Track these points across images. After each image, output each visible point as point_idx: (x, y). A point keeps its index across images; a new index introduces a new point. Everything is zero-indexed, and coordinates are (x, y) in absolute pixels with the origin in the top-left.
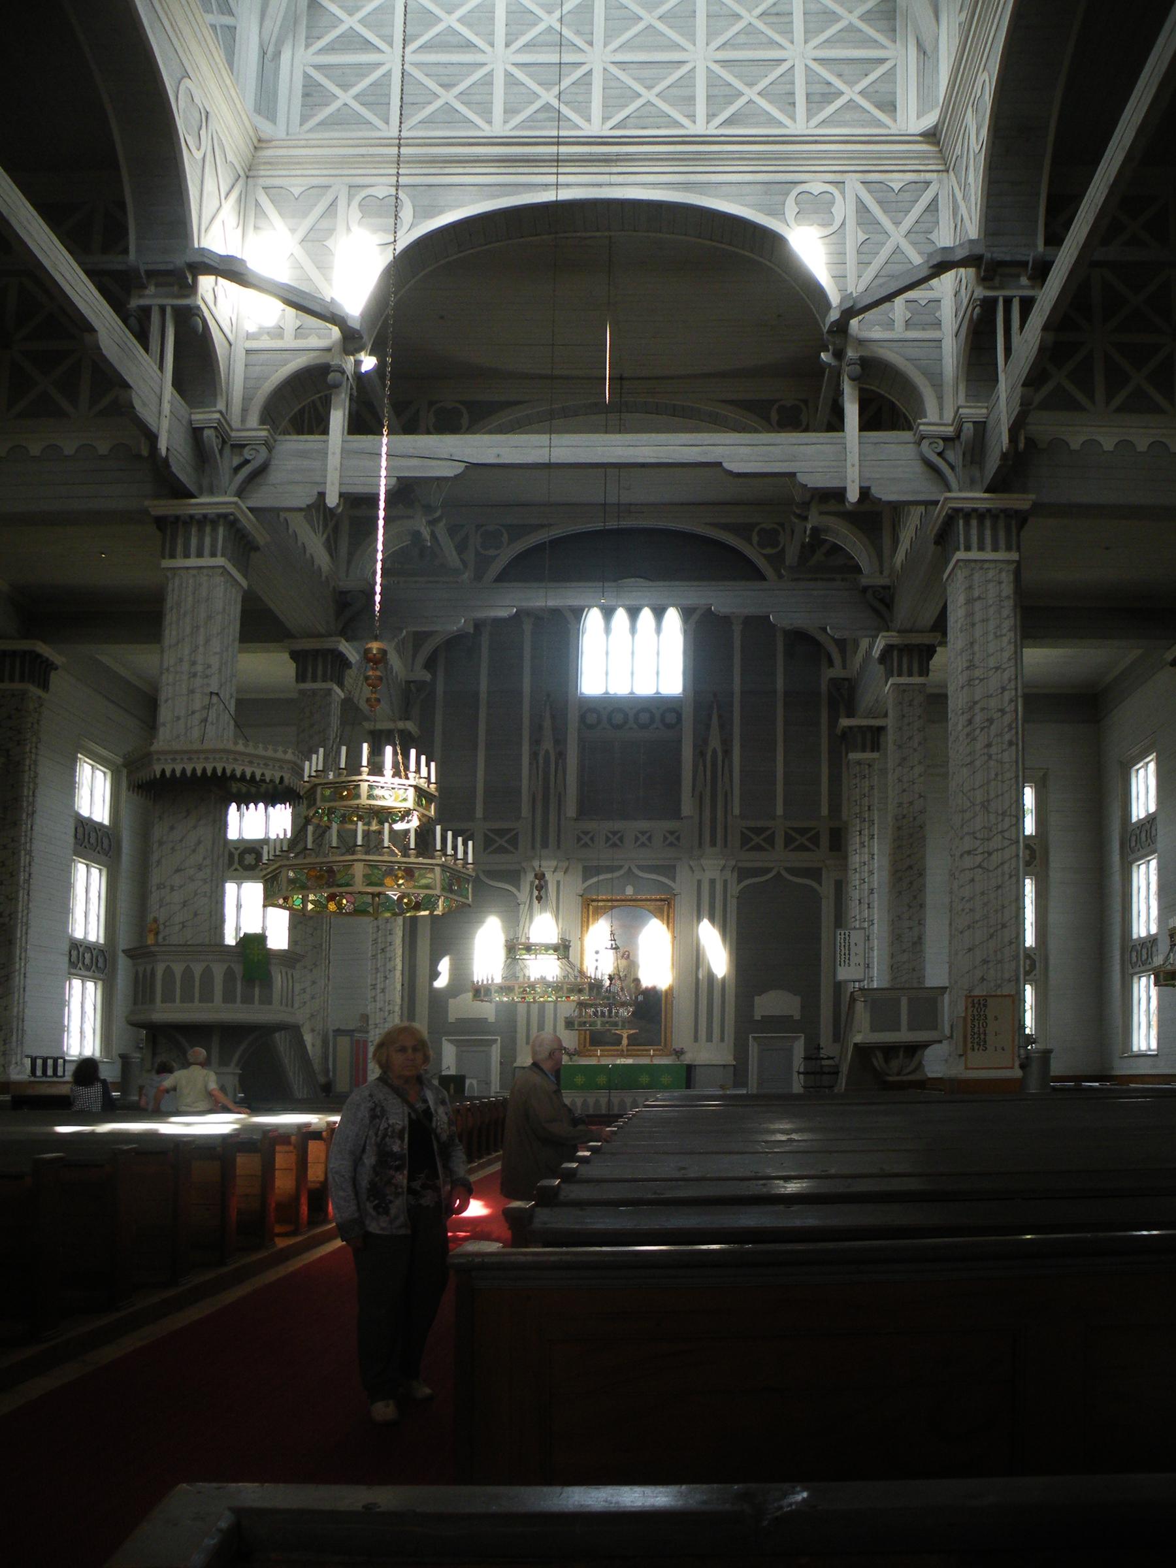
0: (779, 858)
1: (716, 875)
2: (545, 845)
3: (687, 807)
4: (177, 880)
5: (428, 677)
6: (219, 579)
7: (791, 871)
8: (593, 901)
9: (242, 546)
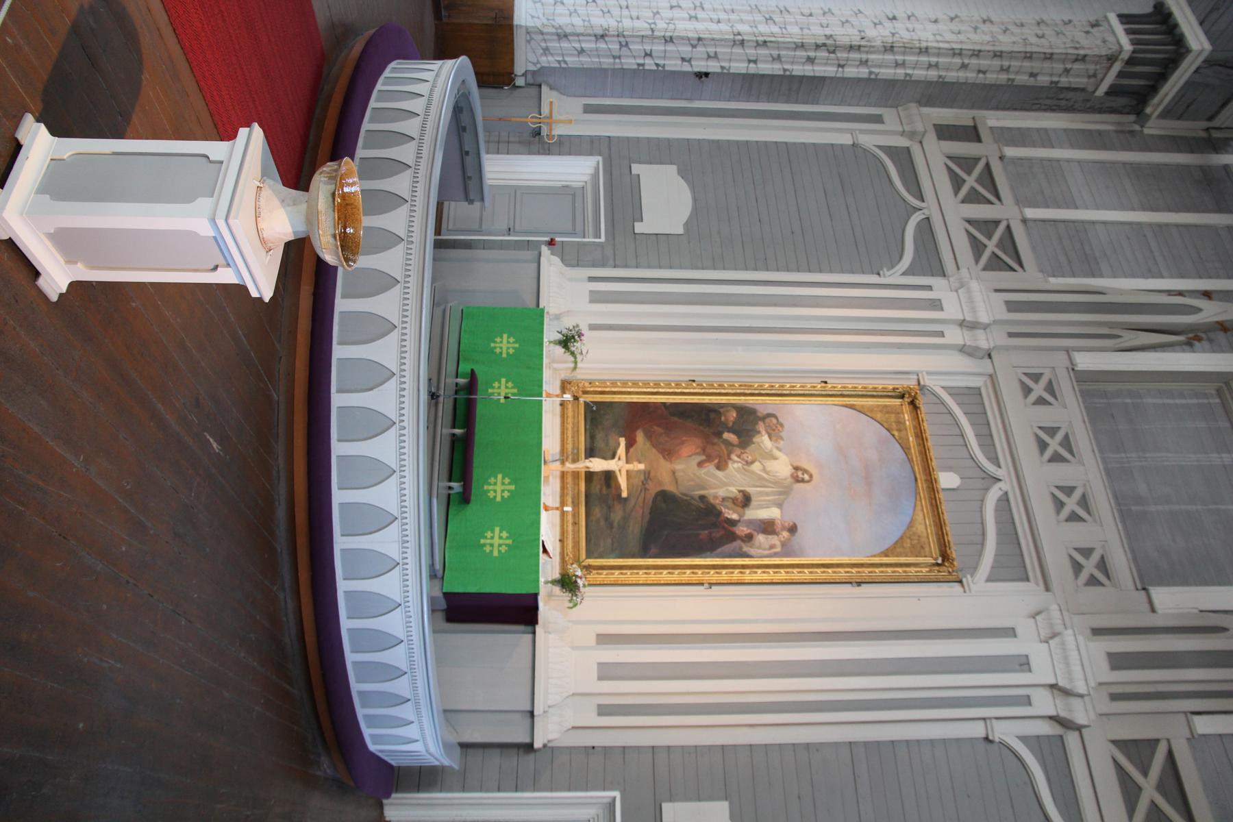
1: (1042, 672)
3: (1173, 601)
8: (913, 403)
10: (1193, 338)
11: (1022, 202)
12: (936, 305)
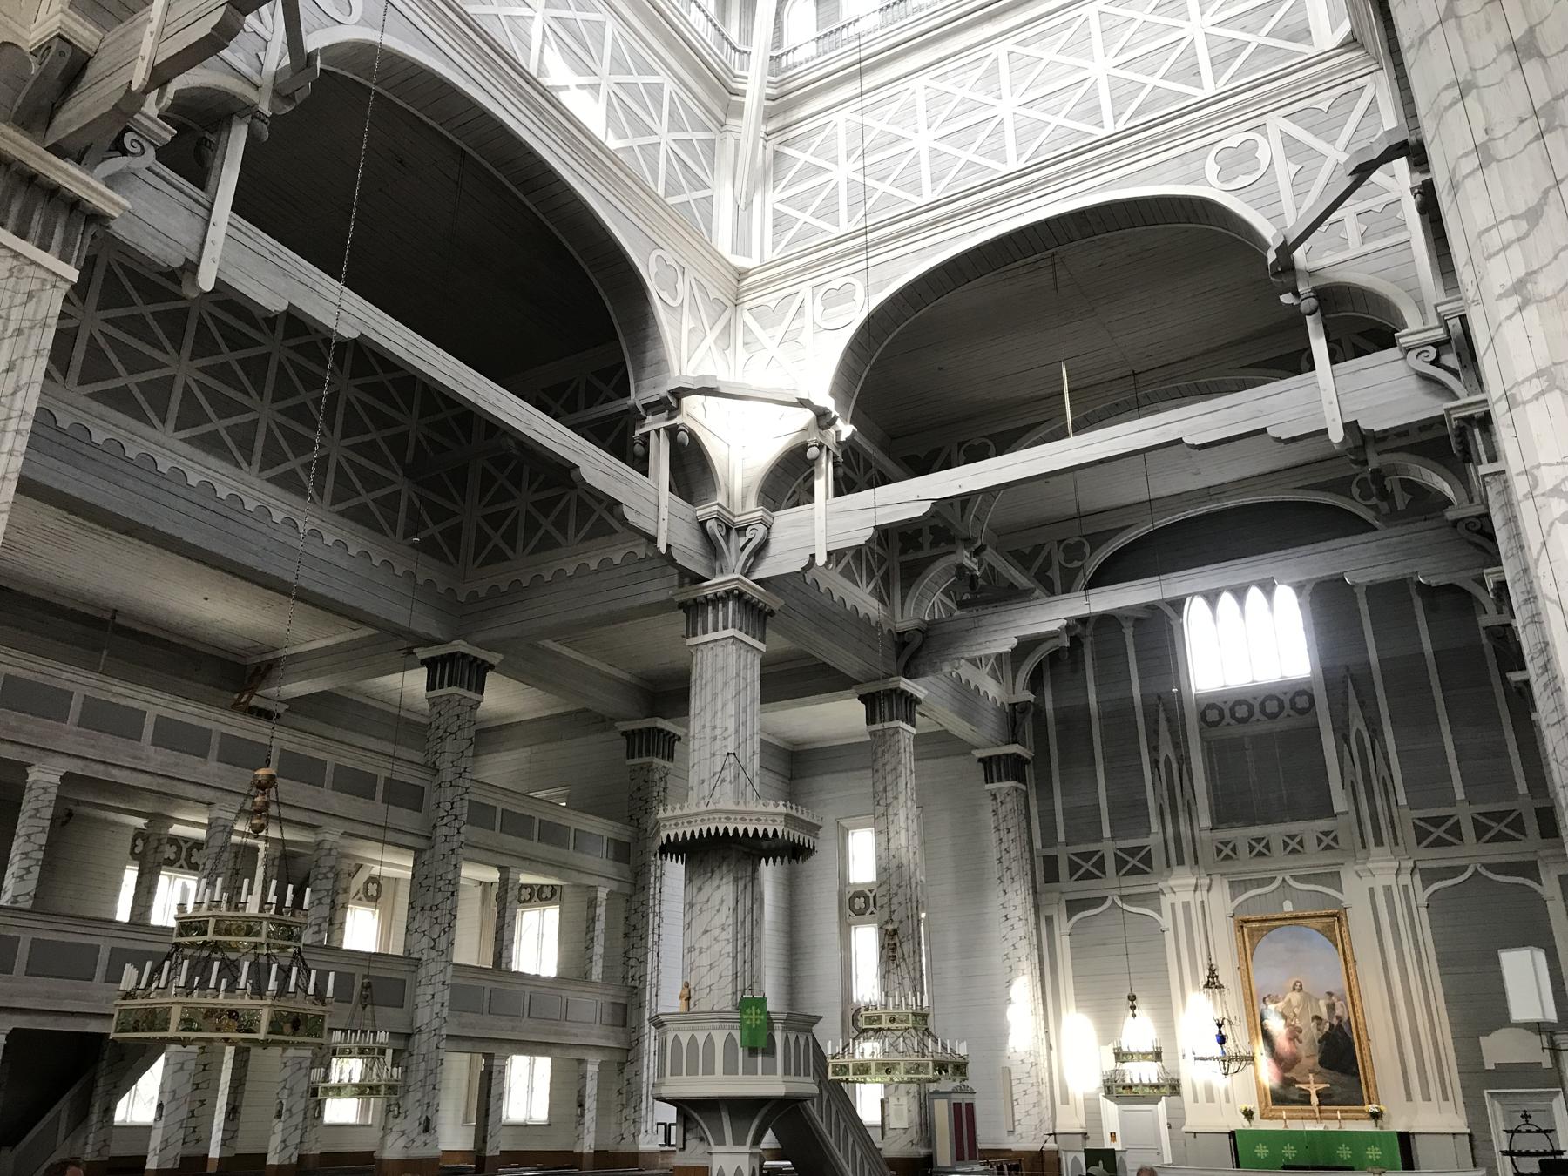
0: (1472, 854)
1: (1390, 880)
2: (1181, 862)
3: (1340, 802)
4: (705, 942)
5: (1031, 697)
6: (732, 649)
7: (1487, 867)
9: (755, 614)
10: (1184, 761)
11: (1100, 839)
12: (1186, 905)
